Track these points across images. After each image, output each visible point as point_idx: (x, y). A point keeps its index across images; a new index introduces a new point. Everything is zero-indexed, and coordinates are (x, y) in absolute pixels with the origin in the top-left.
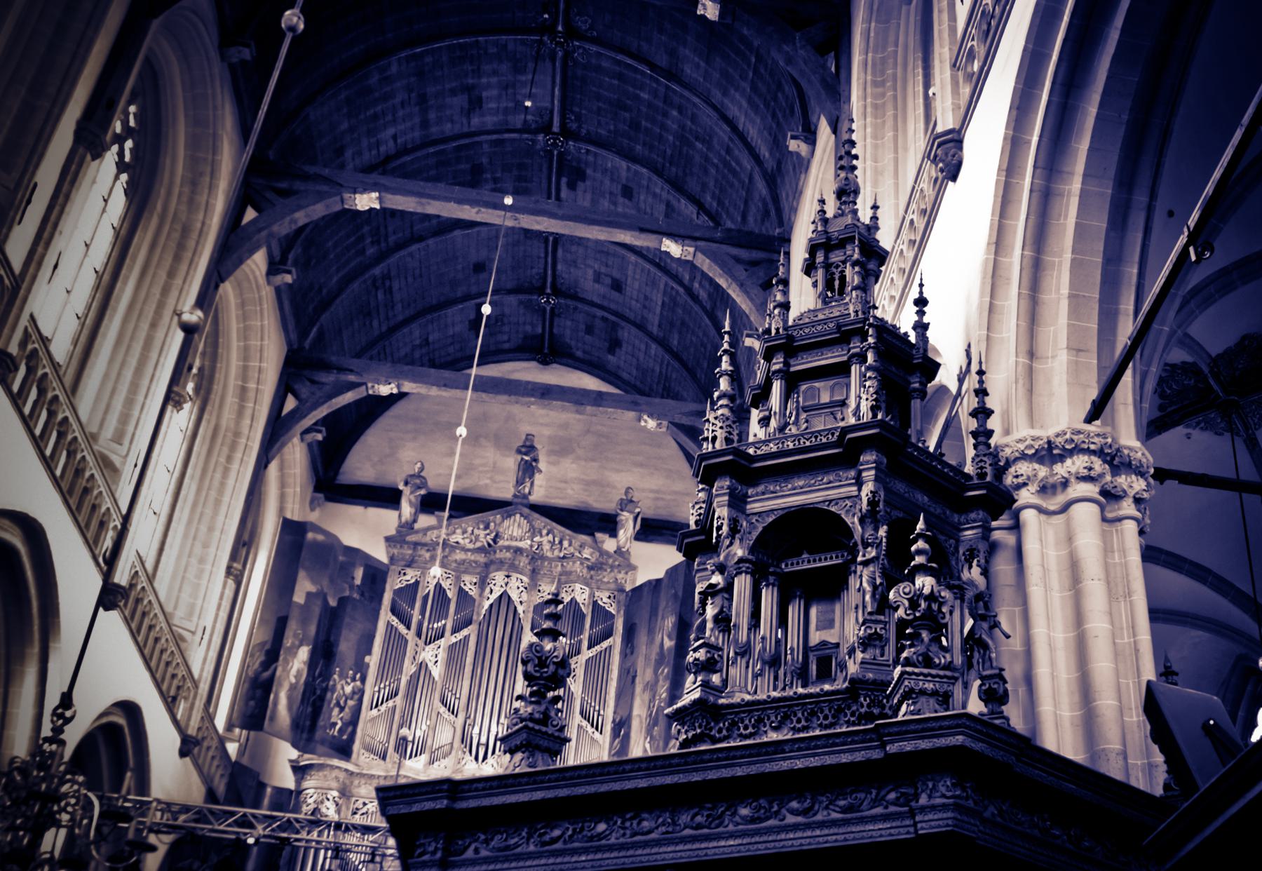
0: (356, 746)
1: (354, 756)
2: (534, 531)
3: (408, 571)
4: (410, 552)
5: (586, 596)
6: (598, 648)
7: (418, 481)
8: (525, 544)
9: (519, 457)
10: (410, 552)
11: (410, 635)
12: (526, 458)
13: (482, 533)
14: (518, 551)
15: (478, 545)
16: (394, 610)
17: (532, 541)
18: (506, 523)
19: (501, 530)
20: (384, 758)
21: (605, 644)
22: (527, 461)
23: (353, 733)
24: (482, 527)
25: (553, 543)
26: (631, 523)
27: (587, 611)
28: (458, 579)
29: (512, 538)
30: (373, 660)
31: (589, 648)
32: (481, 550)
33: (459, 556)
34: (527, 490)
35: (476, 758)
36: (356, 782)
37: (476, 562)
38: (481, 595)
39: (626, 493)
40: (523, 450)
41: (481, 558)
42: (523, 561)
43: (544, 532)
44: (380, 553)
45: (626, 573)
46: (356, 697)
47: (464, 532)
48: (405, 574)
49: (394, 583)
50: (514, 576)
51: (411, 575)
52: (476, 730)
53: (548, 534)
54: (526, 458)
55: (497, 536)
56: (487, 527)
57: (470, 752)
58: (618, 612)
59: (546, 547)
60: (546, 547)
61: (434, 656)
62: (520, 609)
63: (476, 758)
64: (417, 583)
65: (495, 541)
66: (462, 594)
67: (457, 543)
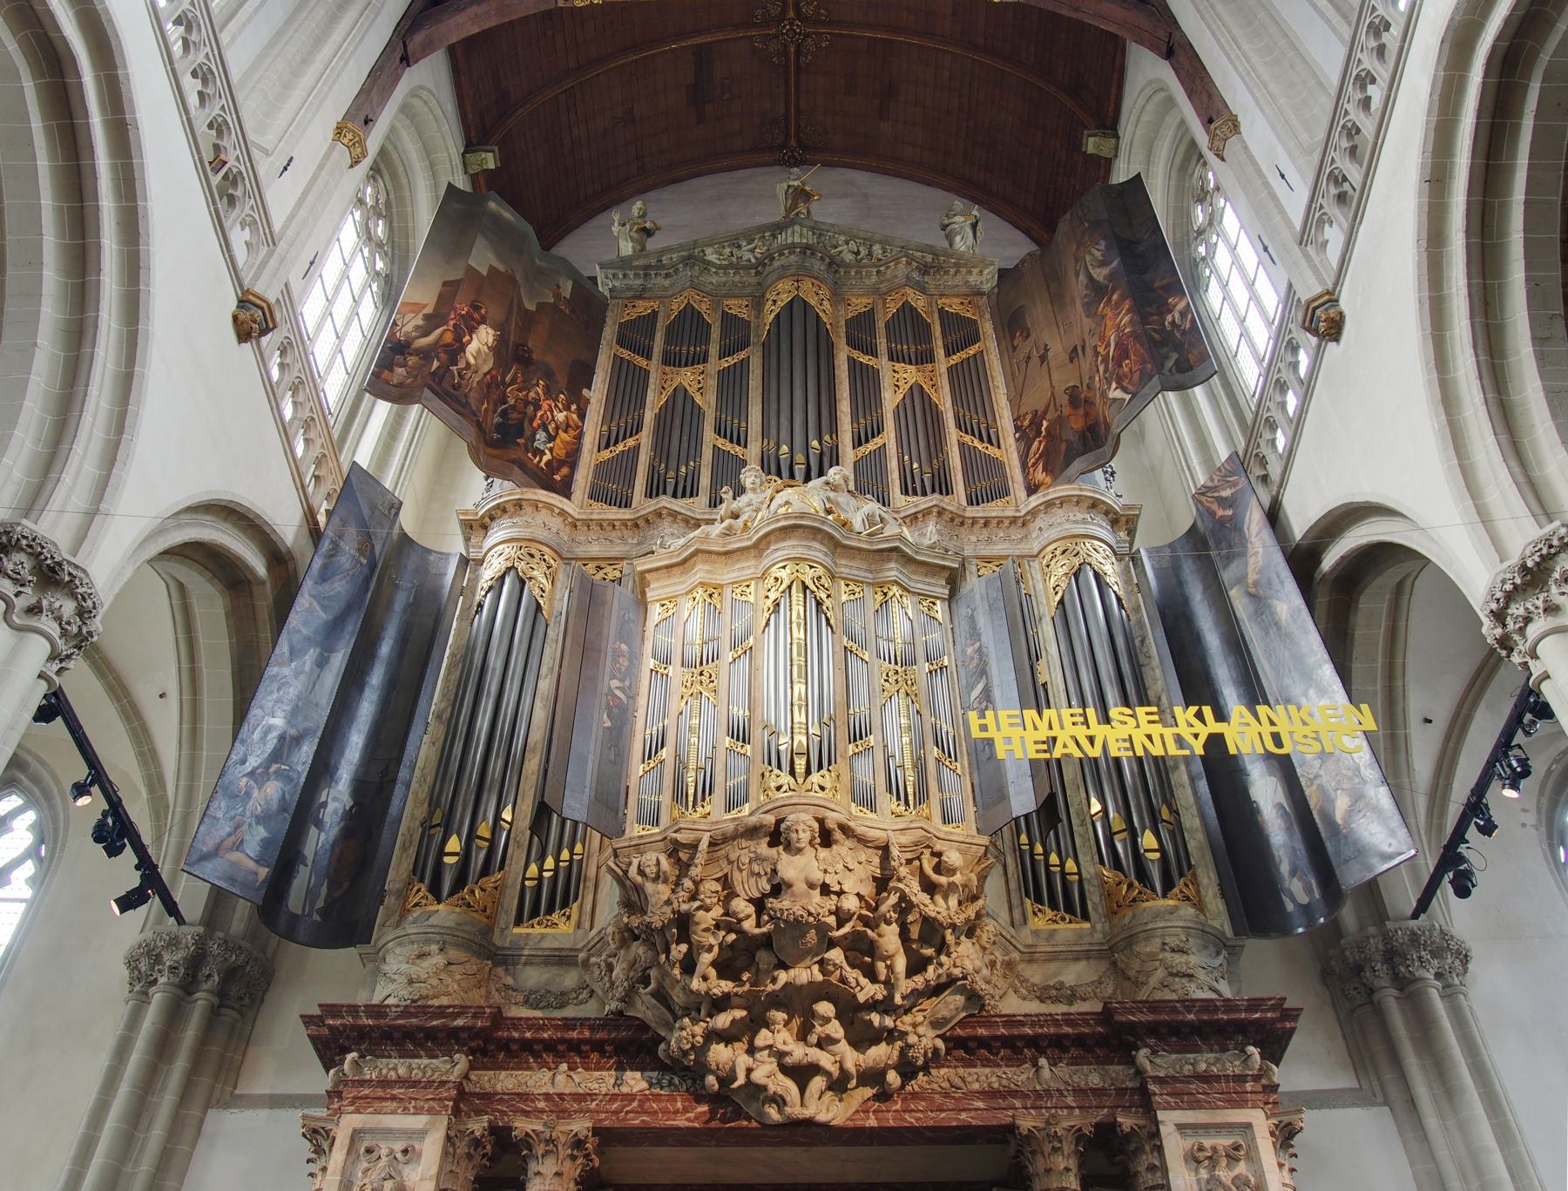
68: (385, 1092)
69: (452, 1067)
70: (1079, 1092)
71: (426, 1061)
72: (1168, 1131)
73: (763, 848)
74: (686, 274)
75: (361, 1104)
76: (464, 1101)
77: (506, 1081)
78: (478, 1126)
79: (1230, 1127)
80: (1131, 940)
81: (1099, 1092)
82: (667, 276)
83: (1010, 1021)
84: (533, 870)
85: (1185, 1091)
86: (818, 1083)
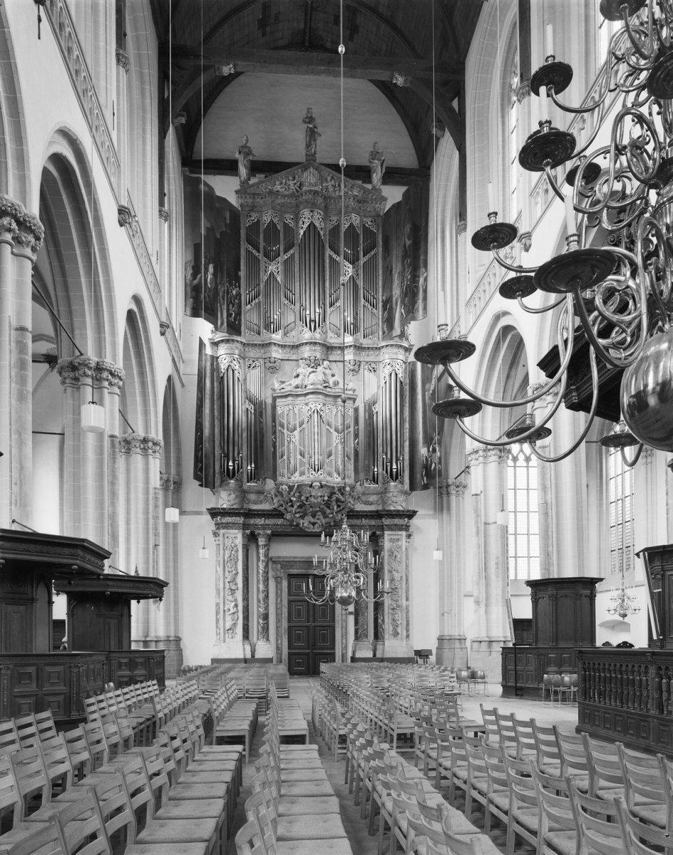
0: (243, 328)
1: (242, 334)
2: (322, 179)
3: (252, 214)
4: (251, 200)
5: (358, 222)
6: (368, 256)
7: (246, 150)
8: (318, 188)
9: (305, 126)
10: (251, 200)
11: (261, 256)
12: (311, 126)
13: (291, 183)
14: (316, 193)
15: (291, 191)
16: (248, 241)
17: (322, 186)
18: (305, 174)
19: (303, 180)
20: (259, 334)
21: (373, 253)
22: (311, 128)
23: (240, 320)
24: (291, 178)
25: (335, 186)
26: (379, 168)
27: (360, 231)
28: (282, 218)
29: (310, 184)
30: (242, 274)
31: (364, 256)
32: (292, 195)
33: (280, 201)
34: (313, 150)
35: (310, 329)
36: (246, 349)
37: (290, 203)
38: (297, 226)
39: (374, 146)
40: (307, 120)
41: (293, 201)
42: (320, 200)
43: (329, 178)
44: (233, 200)
45: (380, 204)
46: (238, 297)
47: (281, 183)
48: (250, 216)
49: (245, 223)
50: (316, 211)
51: (254, 217)
52: (308, 312)
53: (331, 180)
54: (311, 126)
55: (300, 184)
56: (294, 179)
57: (306, 325)
58: (378, 231)
59: (331, 189)
60: (331, 189)
61: (275, 268)
62: (322, 233)
63: (310, 329)
64: (258, 221)
65: (300, 187)
66: (286, 226)
67: (278, 191)
68: (227, 526)
69: (241, 520)
70: (370, 526)
71: (235, 518)
72: (386, 535)
73: (308, 488)
74: (269, 199)
75: (224, 528)
76: (245, 526)
77: (252, 521)
78: (248, 532)
79: (398, 535)
80: (386, 493)
81: (374, 526)
82: (262, 198)
83: (357, 511)
84: (249, 468)
85: (391, 528)
86: (317, 525)
